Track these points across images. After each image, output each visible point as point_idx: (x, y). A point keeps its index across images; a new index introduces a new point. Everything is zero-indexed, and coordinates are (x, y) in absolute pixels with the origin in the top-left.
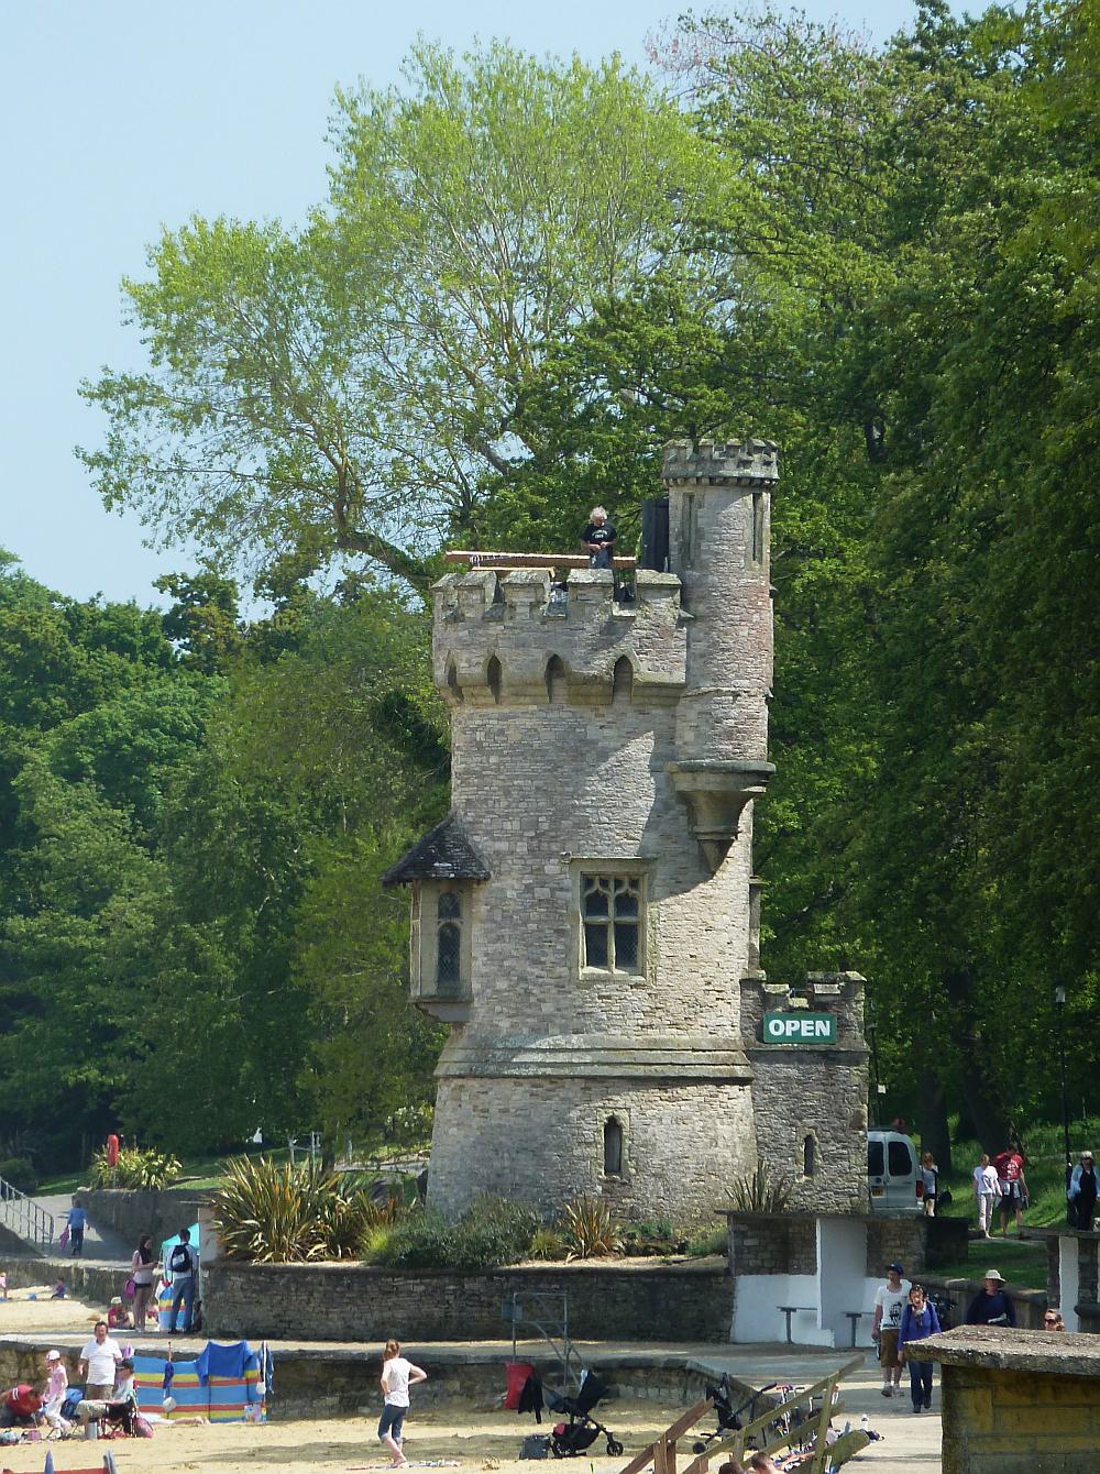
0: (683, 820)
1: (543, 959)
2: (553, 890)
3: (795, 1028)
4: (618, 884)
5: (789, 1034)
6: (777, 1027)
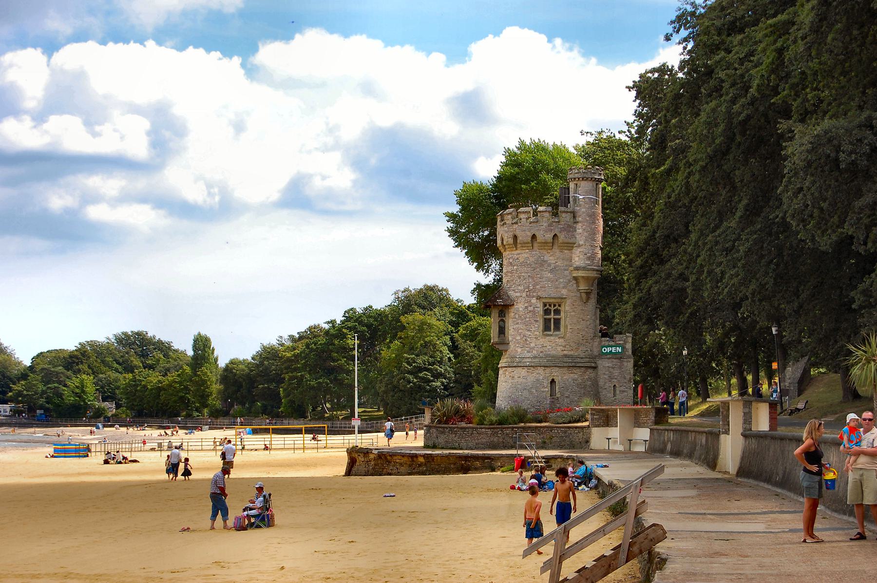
2: (534, 308)
4: (555, 306)
6: (605, 350)
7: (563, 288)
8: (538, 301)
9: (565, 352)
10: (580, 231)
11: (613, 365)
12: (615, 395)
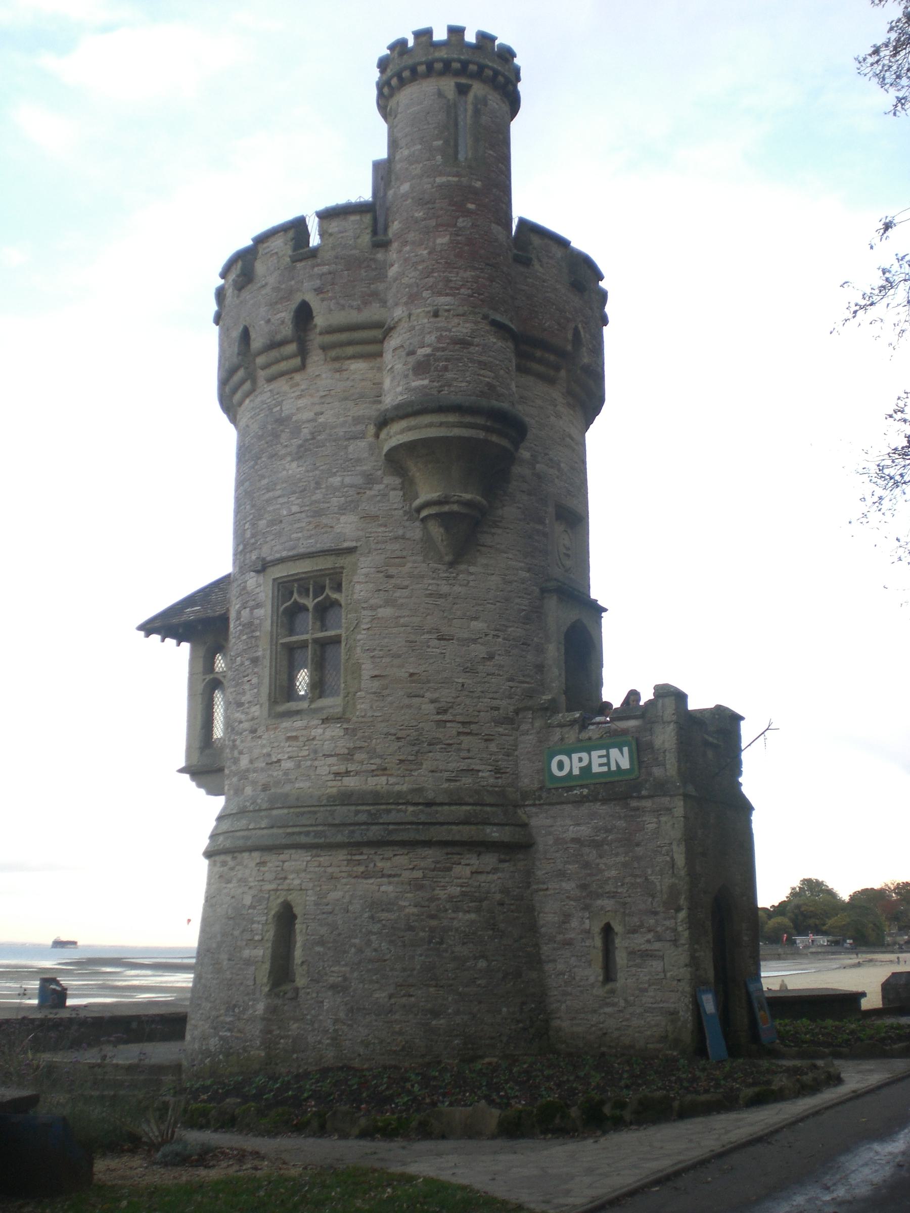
0: (396, 496)
3: (585, 763)
4: (320, 589)
5: (576, 772)
6: (561, 766)
8: (261, 579)
9: (351, 783)
12: (609, 974)
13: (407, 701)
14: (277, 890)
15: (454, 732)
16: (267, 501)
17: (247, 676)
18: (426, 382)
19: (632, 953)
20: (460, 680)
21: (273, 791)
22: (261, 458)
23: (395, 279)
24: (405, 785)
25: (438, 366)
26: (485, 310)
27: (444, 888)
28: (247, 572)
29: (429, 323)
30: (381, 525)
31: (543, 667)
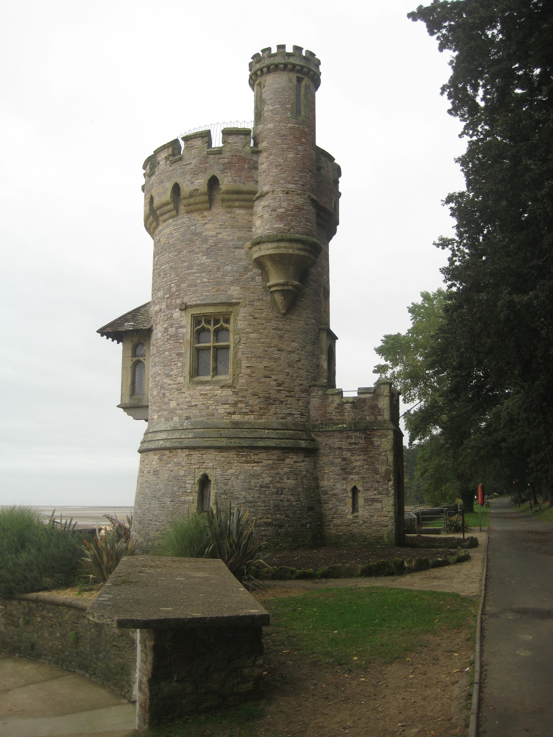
0: (259, 279)
1: (171, 373)
4: (217, 322)
7: (232, 283)
8: (183, 313)
9: (236, 417)
10: (263, 167)
11: (351, 444)
12: (355, 508)
13: (264, 380)
14: (199, 468)
15: (284, 395)
16: (187, 274)
17: (175, 362)
18: (282, 226)
19: (366, 500)
20: (287, 371)
21: (192, 420)
22: (183, 251)
23: (264, 172)
24: (263, 420)
25: (288, 218)
26: (309, 193)
27: (282, 469)
28: (173, 309)
29: (284, 196)
30: (251, 293)
31: (319, 366)
